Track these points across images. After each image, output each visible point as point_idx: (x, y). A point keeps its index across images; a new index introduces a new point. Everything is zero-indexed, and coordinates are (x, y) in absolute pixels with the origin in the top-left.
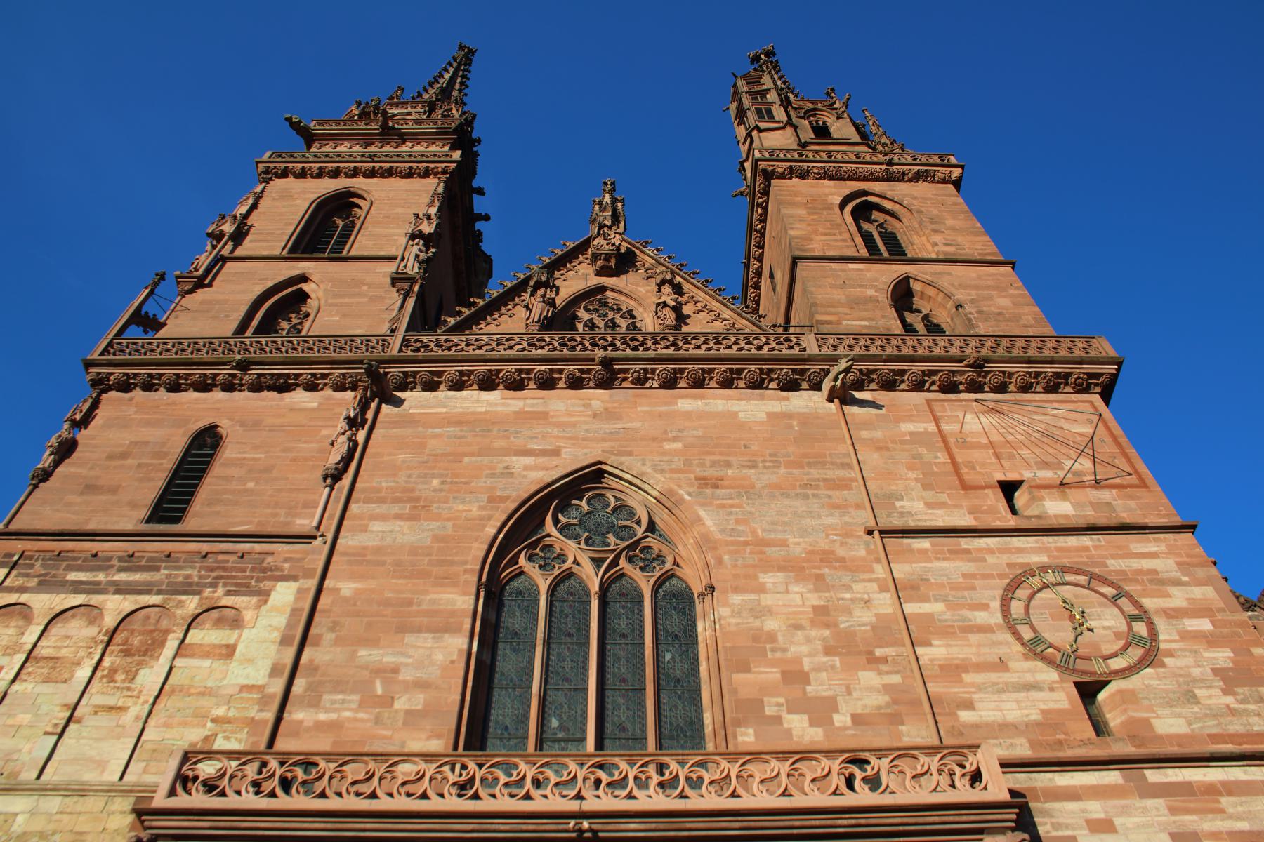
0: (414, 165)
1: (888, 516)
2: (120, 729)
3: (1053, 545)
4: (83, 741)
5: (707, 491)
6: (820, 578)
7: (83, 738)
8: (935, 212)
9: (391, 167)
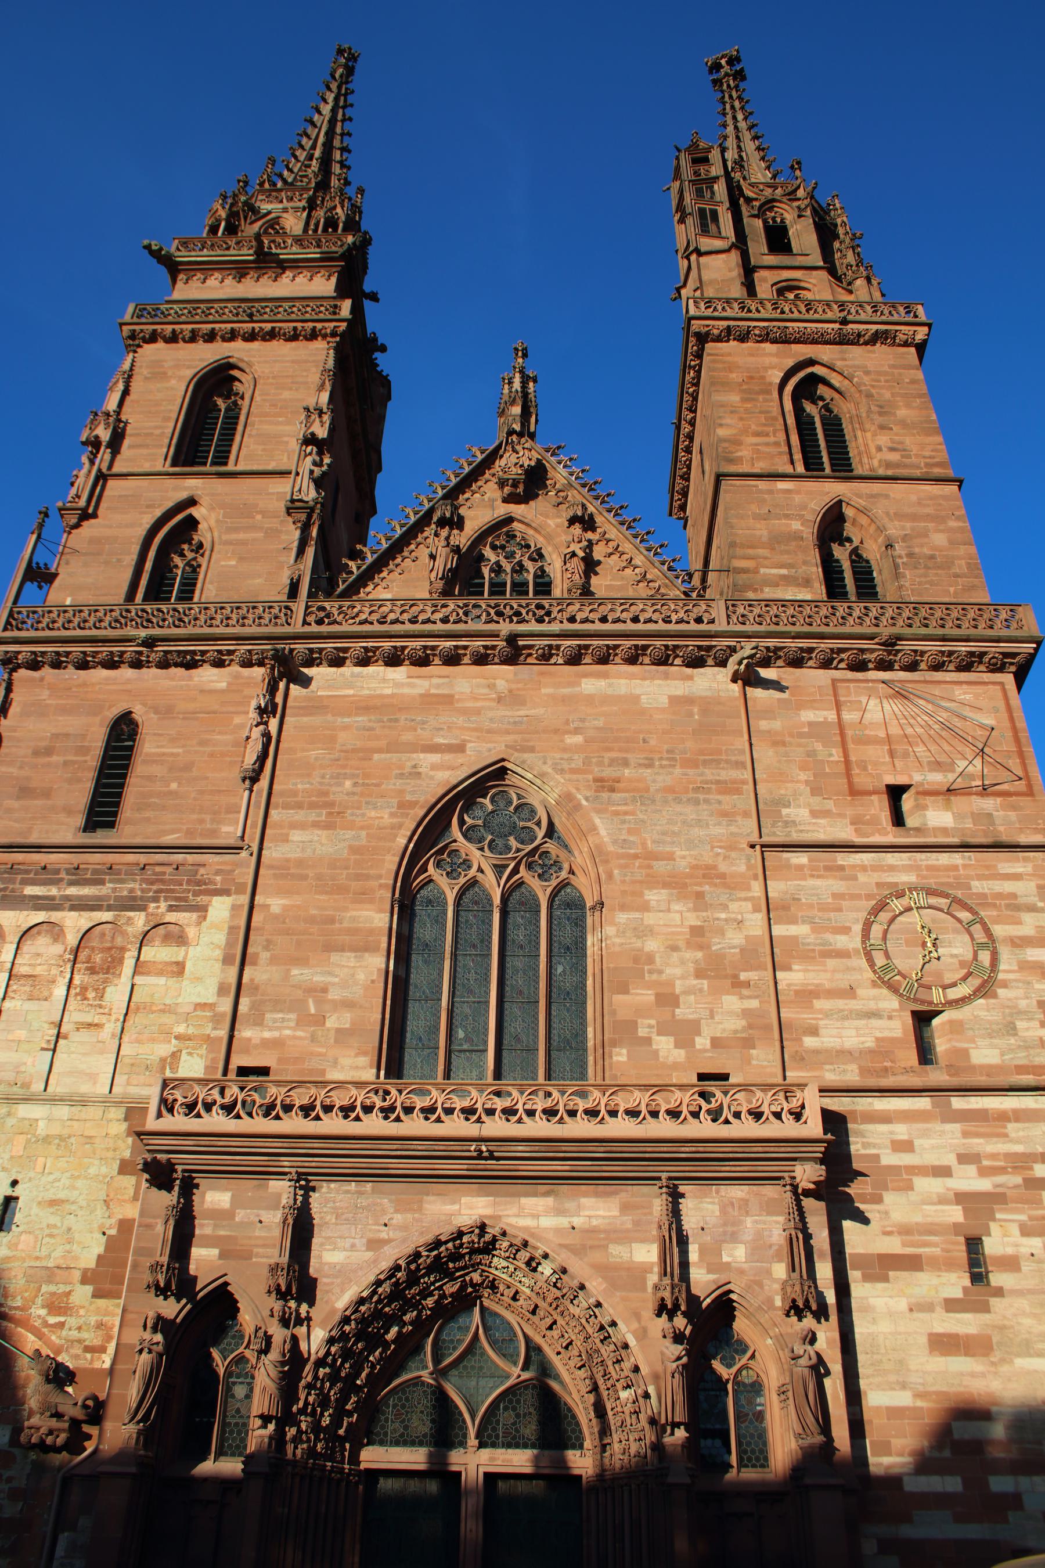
0: (299, 325)
1: (773, 826)
2: (101, 1045)
3: (924, 863)
4: (73, 1056)
5: (603, 795)
6: (700, 895)
7: (73, 1053)
8: (887, 395)
9: (273, 328)
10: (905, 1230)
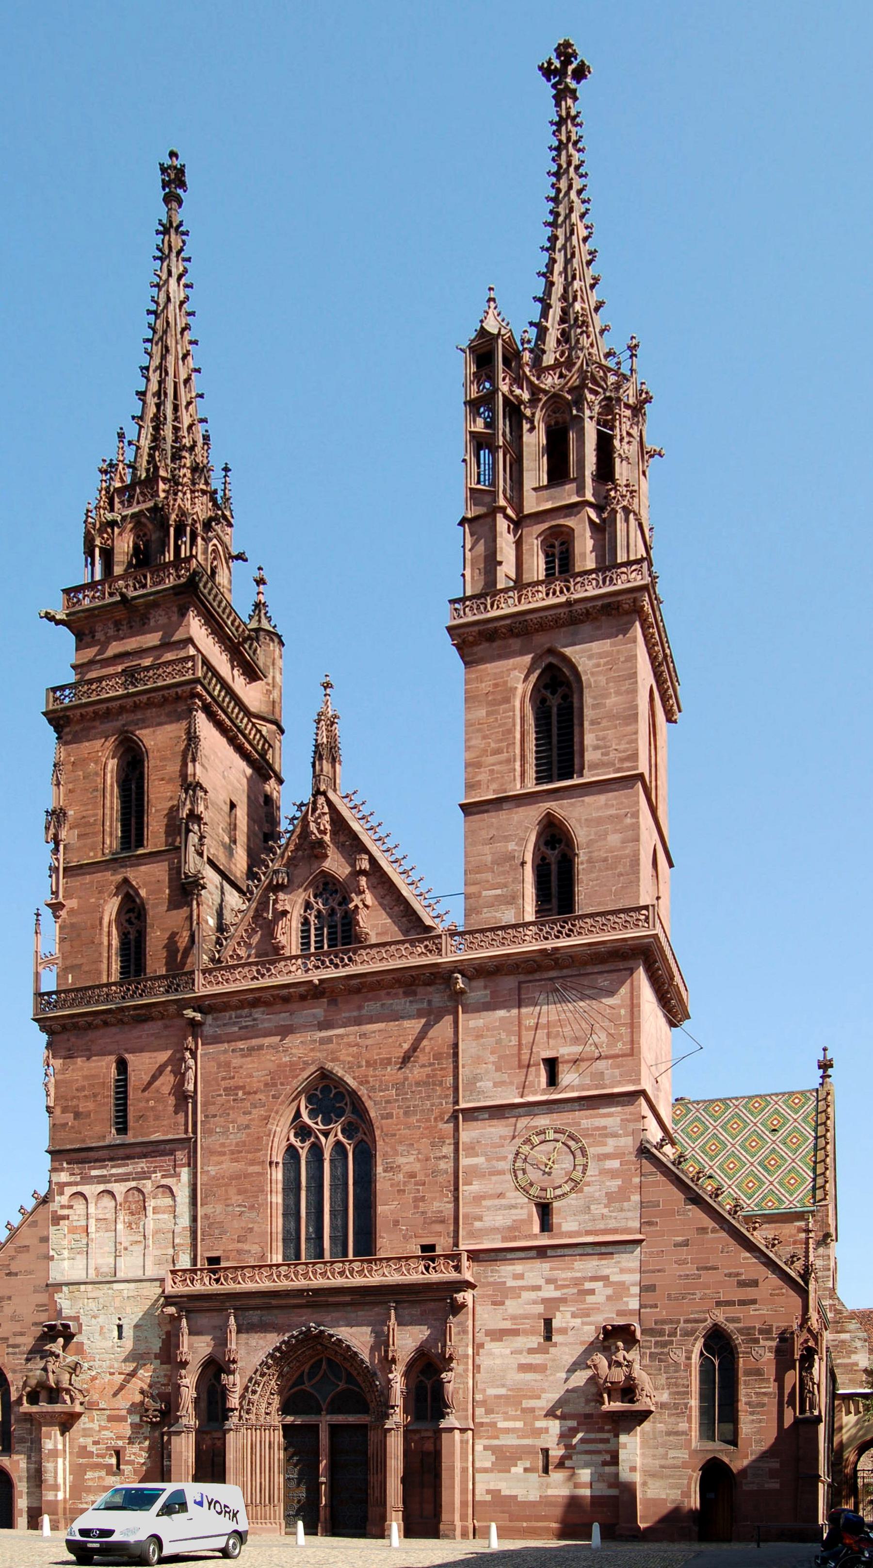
10: (514, 1318)
